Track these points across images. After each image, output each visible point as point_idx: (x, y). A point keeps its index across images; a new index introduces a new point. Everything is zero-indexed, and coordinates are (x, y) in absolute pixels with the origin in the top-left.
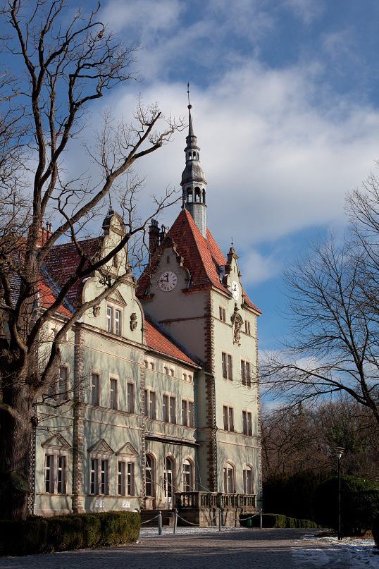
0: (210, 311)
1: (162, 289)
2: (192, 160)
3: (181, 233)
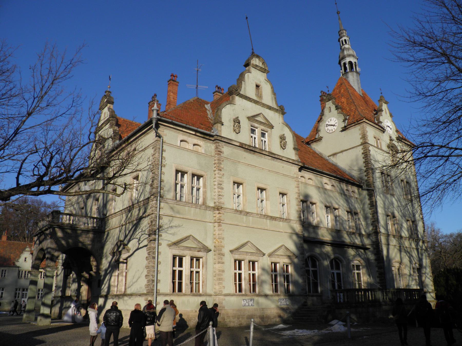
0: (365, 139)
1: (328, 131)
3: (340, 92)
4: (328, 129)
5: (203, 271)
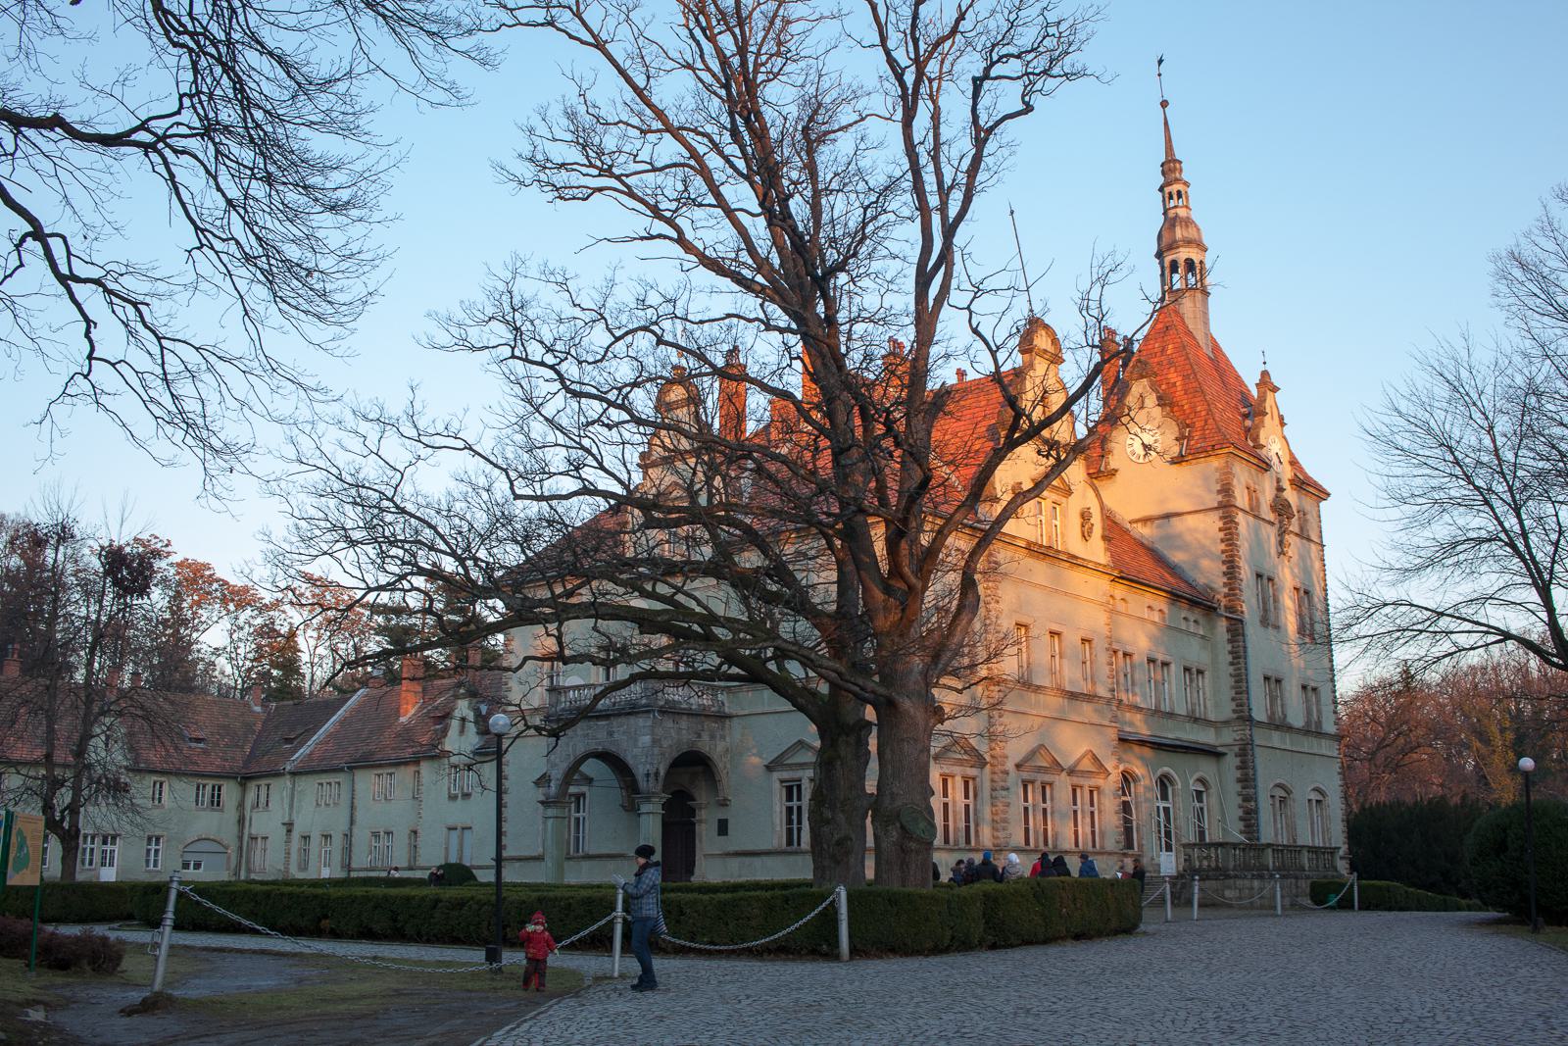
0: (1230, 496)
1: (1133, 458)
2: (1176, 207)
3: (1163, 350)
5: (975, 805)
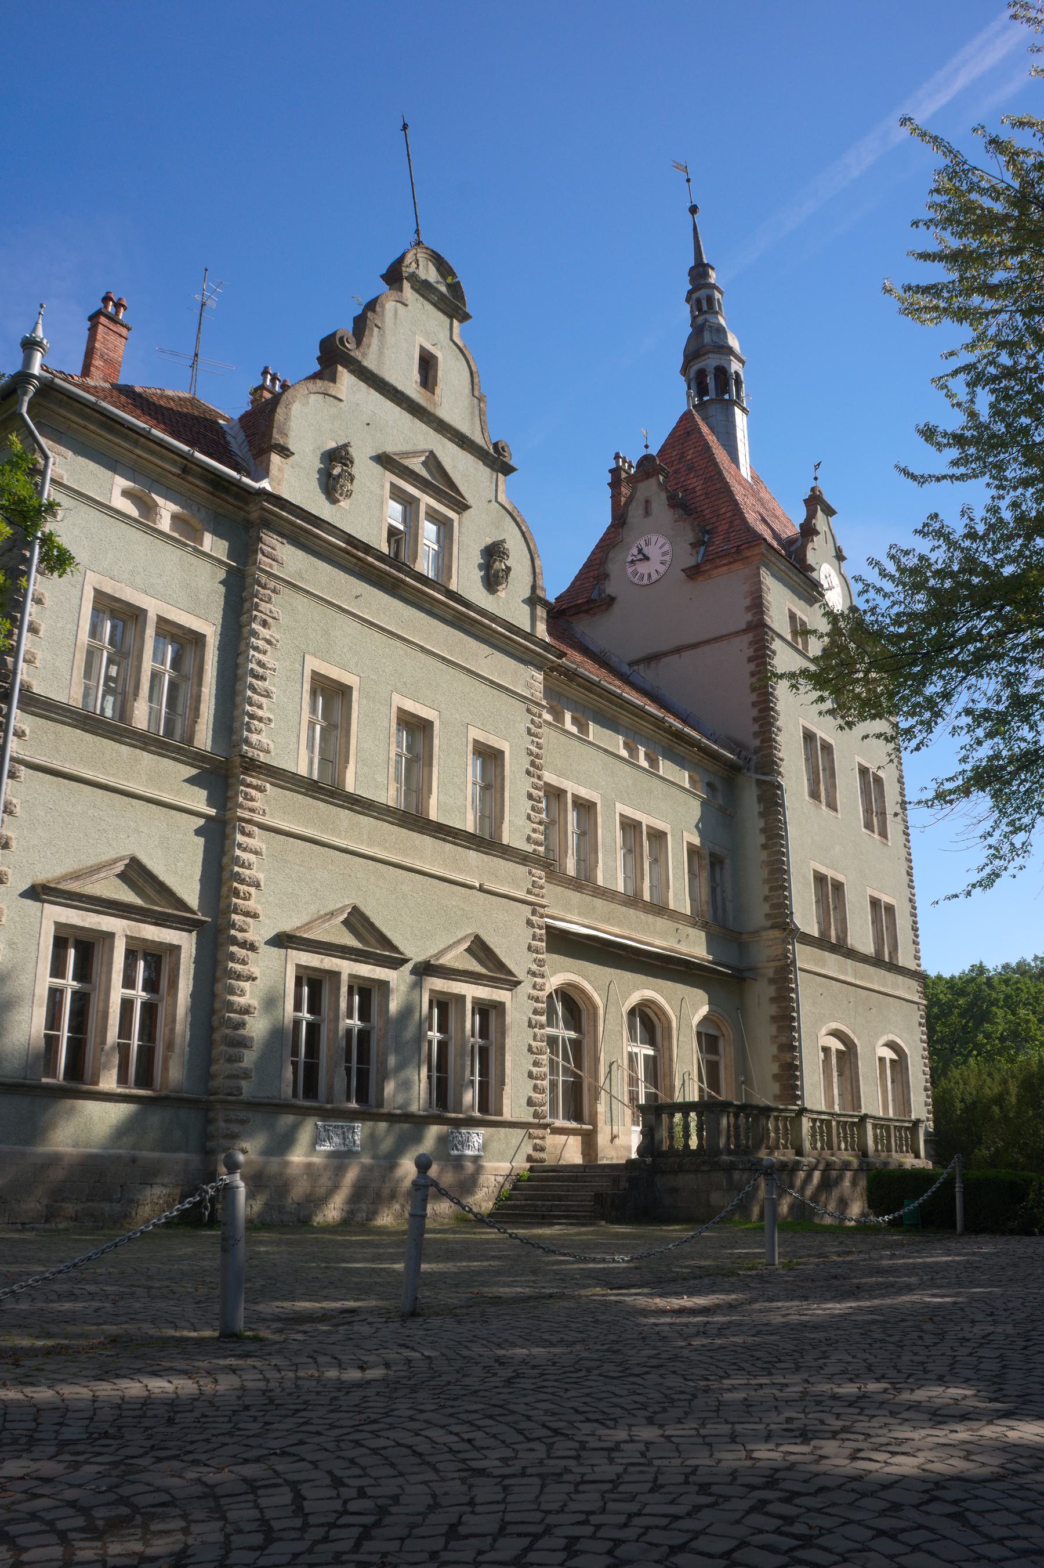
0: (762, 613)
1: (636, 580)
3: (682, 456)
4: (635, 573)
